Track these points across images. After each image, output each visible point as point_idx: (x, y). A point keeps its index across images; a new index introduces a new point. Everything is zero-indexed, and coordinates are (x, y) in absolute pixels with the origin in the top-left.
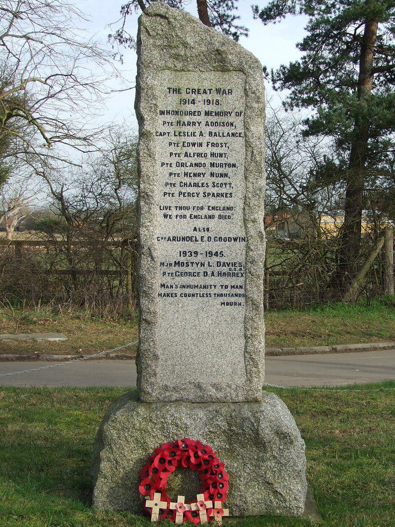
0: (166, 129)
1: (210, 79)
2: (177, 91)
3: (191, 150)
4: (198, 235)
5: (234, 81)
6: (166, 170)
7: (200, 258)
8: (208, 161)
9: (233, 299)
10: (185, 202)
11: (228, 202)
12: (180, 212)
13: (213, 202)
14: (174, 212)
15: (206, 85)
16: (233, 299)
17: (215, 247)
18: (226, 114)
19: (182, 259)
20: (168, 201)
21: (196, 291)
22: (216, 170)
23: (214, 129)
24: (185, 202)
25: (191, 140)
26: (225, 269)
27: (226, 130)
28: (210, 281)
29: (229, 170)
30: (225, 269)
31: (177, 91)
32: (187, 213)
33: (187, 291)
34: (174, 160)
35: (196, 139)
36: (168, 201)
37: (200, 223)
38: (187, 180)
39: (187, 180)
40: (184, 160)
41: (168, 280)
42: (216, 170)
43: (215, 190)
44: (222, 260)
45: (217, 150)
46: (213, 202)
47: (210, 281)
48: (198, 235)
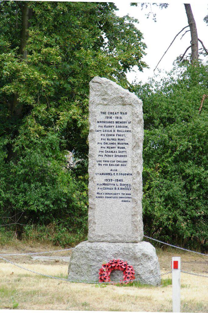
0: (100, 129)
1: (119, 108)
2: (104, 113)
3: (110, 137)
4: (112, 172)
5: (128, 109)
6: (100, 146)
7: (113, 182)
8: (117, 142)
9: (126, 199)
10: (107, 159)
11: (125, 159)
12: (105, 163)
13: (119, 159)
14: (103, 163)
15: (117, 111)
16: (126, 199)
17: (119, 177)
18: (124, 122)
19: (106, 182)
20: (100, 158)
21: (111, 196)
22: (120, 146)
23: (119, 129)
24: (107, 159)
25: (110, 133)
26: (124, 187)
27: (124, 129)
28: (117, 191)
29: (125, 146)
30: (124, 187)
31: (104, 113)
32: (108, 163)
33: (108, 196)
34: (103, 142)
35: (112, 133)
36: (100, 158)
37: (113, 168)
38: (108, 150)
39: (108, 150)
40: (107, 141)
41: (100, 191)
42: (120, 146)
43: (120, 154)
44: (122, 183)
45: (120, 138)
46: (119, 159)
47: (117, 191)
48: (112, 172)
